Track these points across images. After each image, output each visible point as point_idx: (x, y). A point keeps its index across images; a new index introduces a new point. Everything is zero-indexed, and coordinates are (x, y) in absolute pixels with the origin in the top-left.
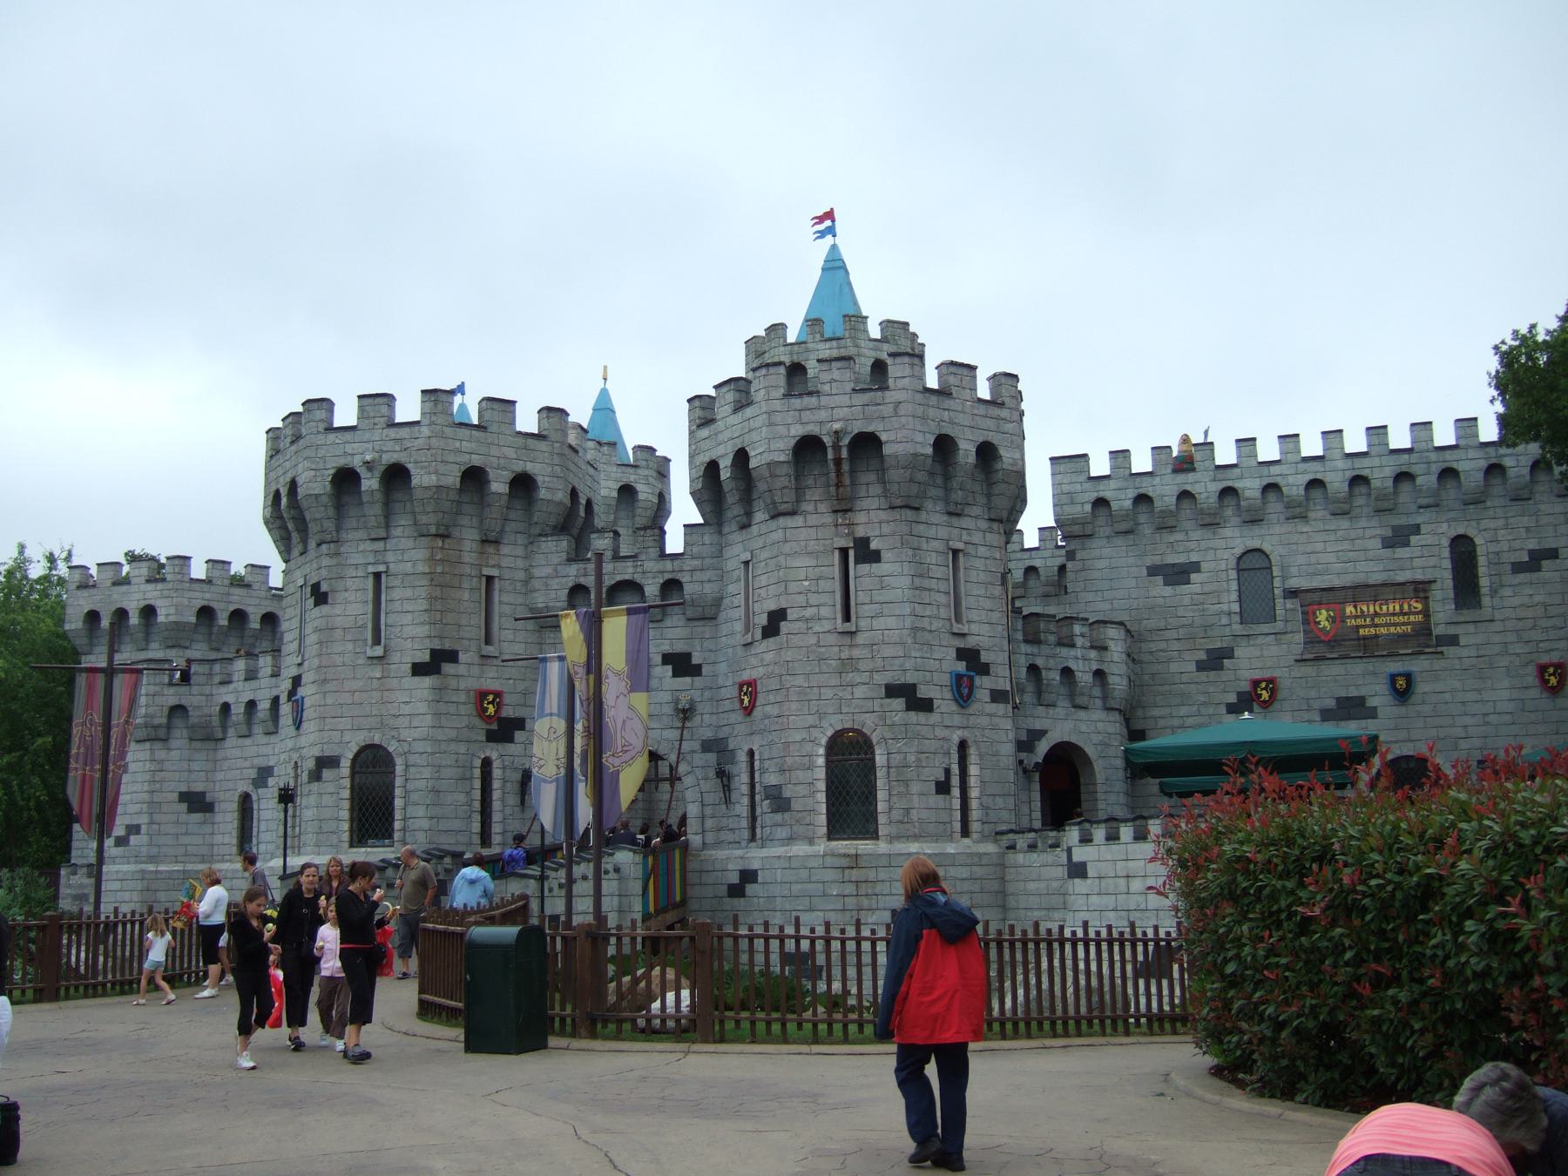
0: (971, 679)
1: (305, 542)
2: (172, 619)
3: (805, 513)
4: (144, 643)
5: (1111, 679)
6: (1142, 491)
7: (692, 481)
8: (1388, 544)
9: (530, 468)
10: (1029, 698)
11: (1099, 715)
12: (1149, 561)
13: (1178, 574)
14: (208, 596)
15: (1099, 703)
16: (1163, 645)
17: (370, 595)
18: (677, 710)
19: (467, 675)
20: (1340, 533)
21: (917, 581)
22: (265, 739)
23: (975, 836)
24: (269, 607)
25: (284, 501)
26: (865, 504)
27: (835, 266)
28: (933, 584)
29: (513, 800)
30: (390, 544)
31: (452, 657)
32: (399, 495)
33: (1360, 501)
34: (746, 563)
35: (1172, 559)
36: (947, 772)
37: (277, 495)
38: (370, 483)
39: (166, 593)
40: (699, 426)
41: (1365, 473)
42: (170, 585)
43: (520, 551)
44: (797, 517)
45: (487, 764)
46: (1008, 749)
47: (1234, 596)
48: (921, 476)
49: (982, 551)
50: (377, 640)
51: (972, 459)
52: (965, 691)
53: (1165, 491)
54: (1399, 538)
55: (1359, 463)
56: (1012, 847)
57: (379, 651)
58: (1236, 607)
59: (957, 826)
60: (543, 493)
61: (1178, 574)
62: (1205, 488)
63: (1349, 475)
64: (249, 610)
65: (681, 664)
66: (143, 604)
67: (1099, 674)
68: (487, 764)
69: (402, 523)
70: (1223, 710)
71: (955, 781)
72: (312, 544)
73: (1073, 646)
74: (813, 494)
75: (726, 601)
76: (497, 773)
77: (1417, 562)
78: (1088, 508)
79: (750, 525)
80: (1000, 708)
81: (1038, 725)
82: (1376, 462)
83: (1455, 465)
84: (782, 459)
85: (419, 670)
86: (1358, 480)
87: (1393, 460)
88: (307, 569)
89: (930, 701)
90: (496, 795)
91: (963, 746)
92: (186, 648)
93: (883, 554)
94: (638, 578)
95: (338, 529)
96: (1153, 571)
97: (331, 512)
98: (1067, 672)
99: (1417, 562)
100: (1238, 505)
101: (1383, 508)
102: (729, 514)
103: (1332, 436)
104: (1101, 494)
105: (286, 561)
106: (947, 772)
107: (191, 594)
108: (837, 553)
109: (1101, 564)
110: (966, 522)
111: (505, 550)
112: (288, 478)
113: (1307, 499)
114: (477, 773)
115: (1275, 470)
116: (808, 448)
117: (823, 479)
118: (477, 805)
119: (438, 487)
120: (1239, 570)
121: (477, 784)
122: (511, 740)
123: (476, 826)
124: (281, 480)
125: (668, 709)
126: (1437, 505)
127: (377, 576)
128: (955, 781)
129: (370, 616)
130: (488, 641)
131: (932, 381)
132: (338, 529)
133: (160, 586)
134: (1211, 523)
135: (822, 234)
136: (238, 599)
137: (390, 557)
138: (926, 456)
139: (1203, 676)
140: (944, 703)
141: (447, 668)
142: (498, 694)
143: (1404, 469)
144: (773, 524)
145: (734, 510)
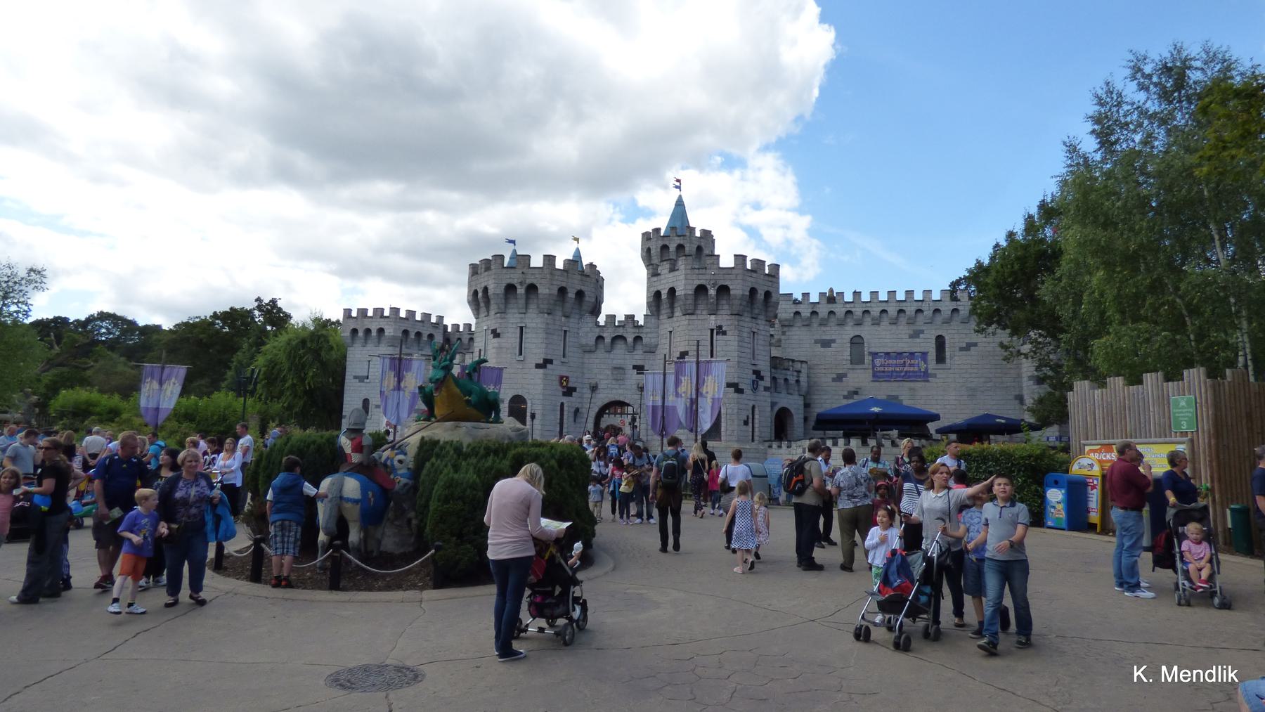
0: (757, 381)
1: (488, 312)
2: (392, 334)
3: (697, 315)
5: (802, 384)
6: (814, 310)
7: (648, 298)
8: (911, 337)
9: (583, 288)
10: (772, 390)
11: (796, 397)
12: (815, 337)
13: (826, 344)
14: (406, 325)
15: (797, 393)
16: (819, 371)
17: (518, 335)
18: (638, 387)
19: (556, 370)
20: (893, 331)
21: (740, 343)
23: (756, 442)
24: (431, 331)
25: (480, 295)
26: (721, 312)
27: (680, 204)
28: (746, 345)
29: (572, 419)
30: (527, 315)
31: (550, 362)
32: (532, 296)
33: (901, 319)
34: (671, 332)
35: (824, 337)
36: (748, 417)
37: (476, 293)
38: (521, 291)
40: (652, 276)
41: (904, 308)
43: (576, 321)
44: (693, 316)
45: (562, 404)
46: (769, 409)
47: (849, 354)
48: (745, 303)
49: (763, 333)
50: (521, 354)
51: (762, 297)
52: (755, 386)
53: (823, 311)
54: (916, 335)
55: (902, 304)
56: (770, 447)
57: (521, 358)
58: (849, 358)
59: (751, 438)
60: (587, 299)
61: (826, 344)
62: (840, 310)
63: (898, 309)
64: (423, 332)
65: (640, 369)
66: (378, 327)
67: (798, 381)
68: (562, 404)
69: (533, 307)
70: (842, 397)
71: (750, 421)
72: (492, 313)
73: (789, 370)
74: (700, 307)
75: (659, 346)
76: (566, 408)
77: (922, 344)
78: (792, 315)
79: (672, 317)
80: (767, 394)
81: (775, 400)
82: (909, 304)
83: (940, 308)
84: (690, 293)
85: (538, 366)
86: (901, 311)
87: (916, 304)
88: (489, 323)
89: (743, 389)
90: (565, 417)
91: (753, 407)
93: (728, 332)
94: (625, 335)
95: (506, 307)
96: (816, 342)
97: (503, 301)
98: (786, 380)
99: (922, 344)
100: (853, 318)
101: (911, 322)
102: (663, 312)
103: (892, 293)
104: (797, 310)
105: (476, 318)
106: (748, 417)
107: (399, 324)
108: (709, 331)
109: (796, 337)
110: (759, 322)
111: (572, 320)
112: (483, 285)
113: (880, 317)
114: (559, 408)
115: (869, 305)
116: (701, 290)
117: (705, 302)
118: (558, 421)
119: (550, 294)
120: (851, 343)
121: (559, 413)
122: (571, 396)
123: (558, 429)
124: (479, 286)
125: (635, 387)
126: (931, 323)
127: (521, 328)
128: (750, 421)
129: (518, 344)
130: (564, 356)
131: (749, 267)
132: (506, 307)
133: (387, 320)
134: (841, 324)
135: (677, 187)
136: (419, 328)
137: (527, 320)
138: (747, 295)
139: (834, 384)
140: (748, 391)
141: (549, 366)
142: (567, 377)
143: (920, 308)
144: (684, 317)
145: (665, 309)
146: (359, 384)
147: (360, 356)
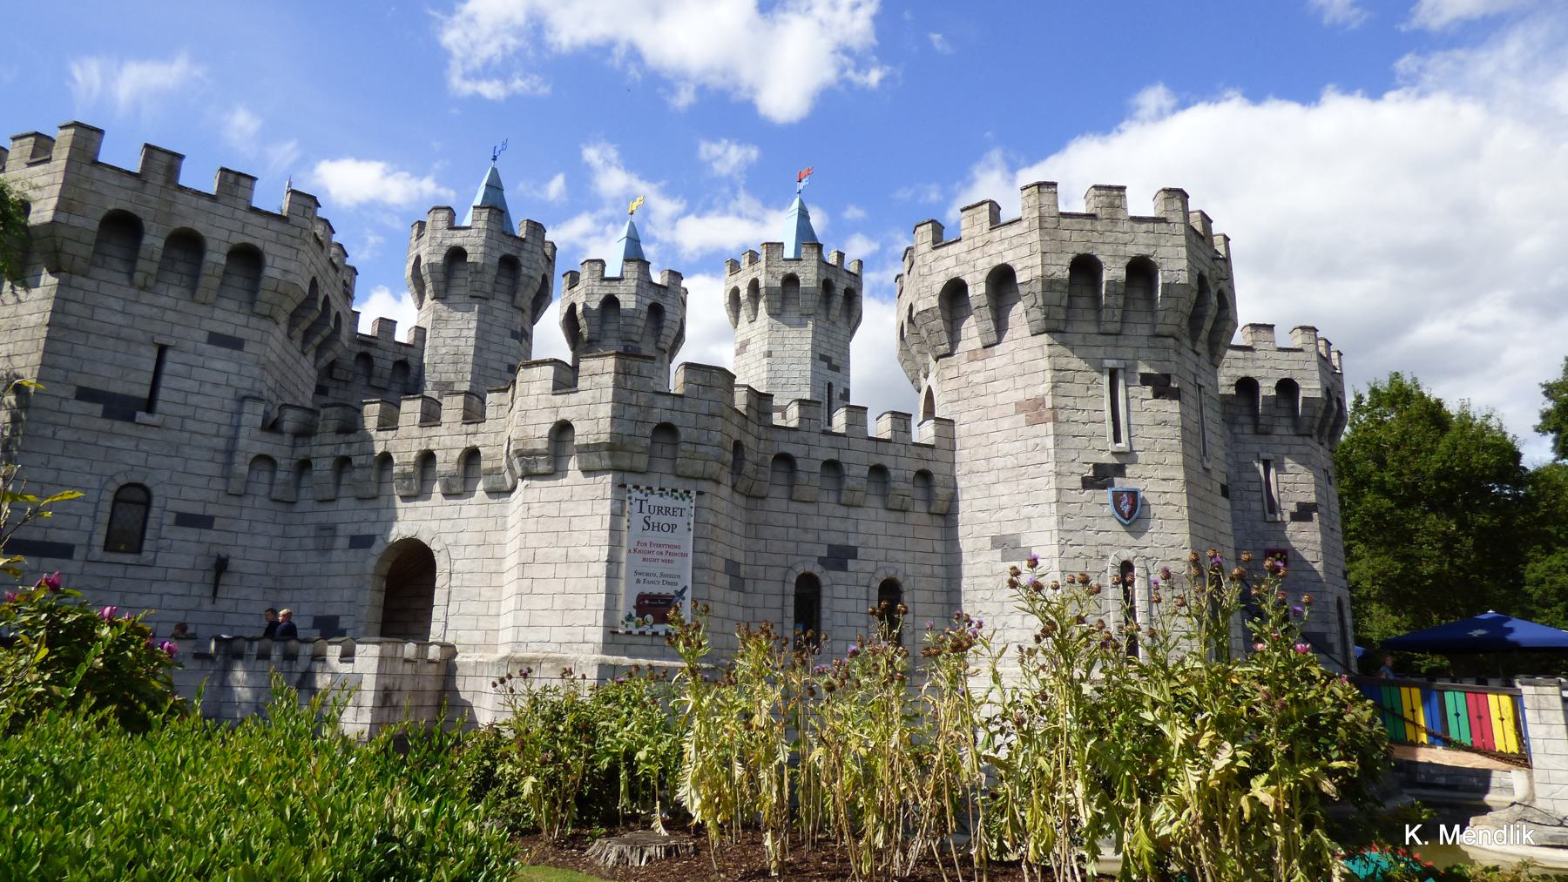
2: (290, 277)
4: (211, 297)
22: (842, 511)
39: (289, 240)
42: (296, 232)
66: (238, 239)
88: (1129, 353)
92: (277, 323)
144: (1299, 440)
146: (105, 424)
147: (119, 319)
